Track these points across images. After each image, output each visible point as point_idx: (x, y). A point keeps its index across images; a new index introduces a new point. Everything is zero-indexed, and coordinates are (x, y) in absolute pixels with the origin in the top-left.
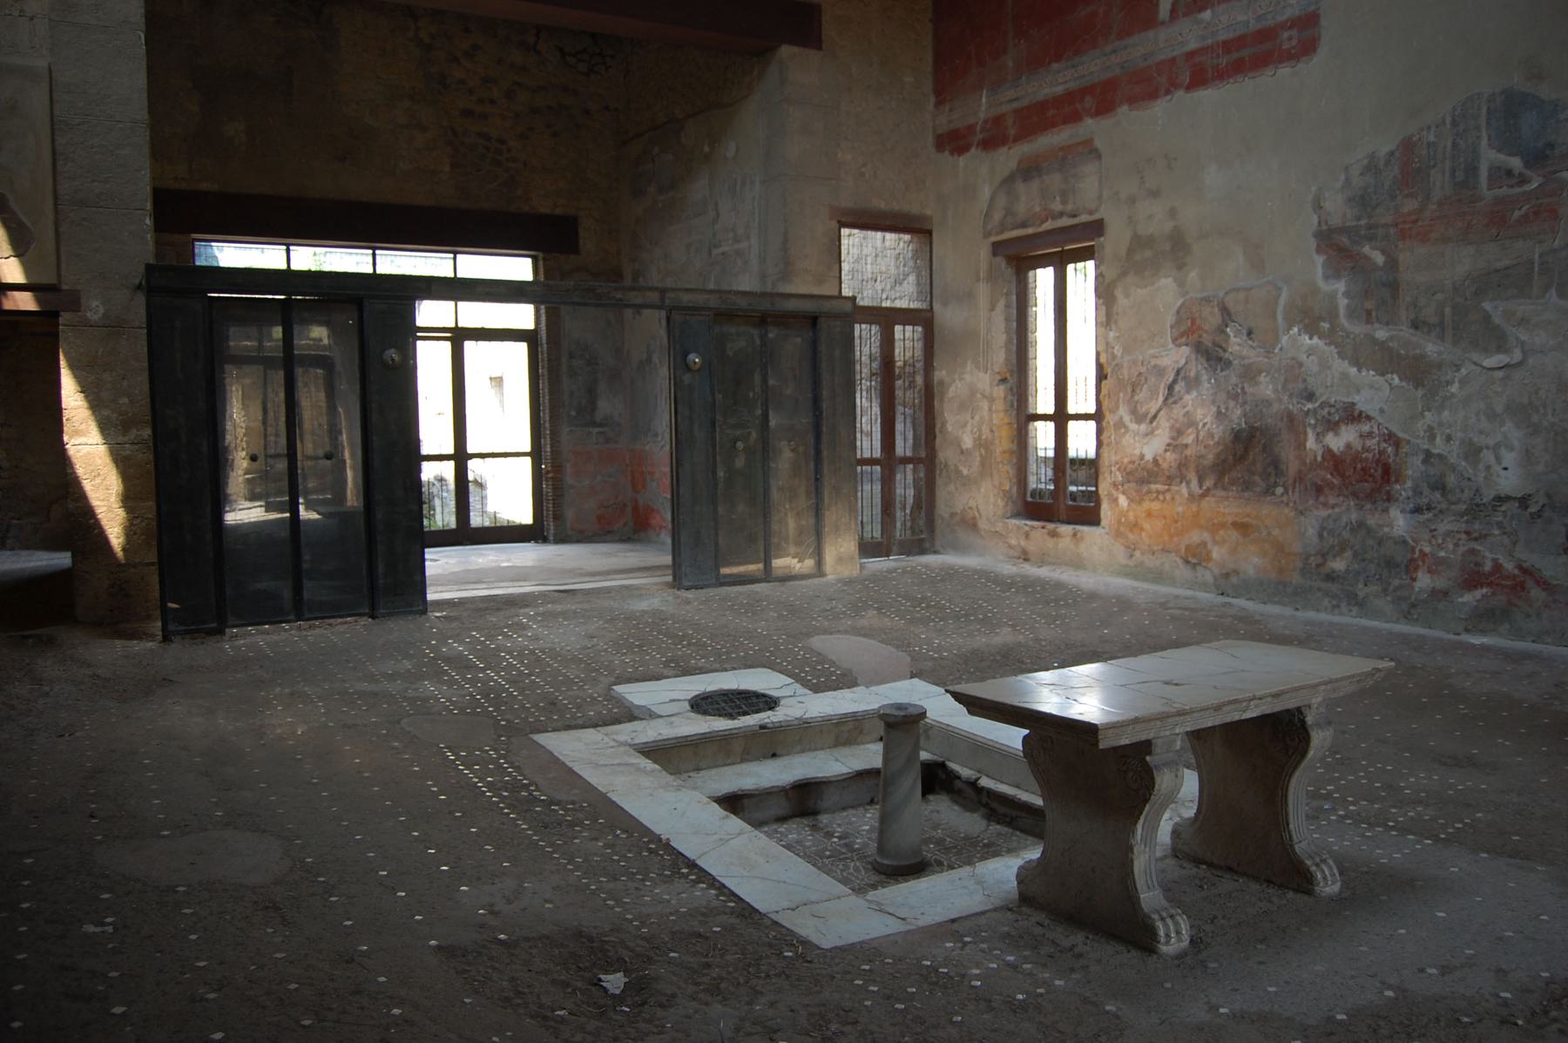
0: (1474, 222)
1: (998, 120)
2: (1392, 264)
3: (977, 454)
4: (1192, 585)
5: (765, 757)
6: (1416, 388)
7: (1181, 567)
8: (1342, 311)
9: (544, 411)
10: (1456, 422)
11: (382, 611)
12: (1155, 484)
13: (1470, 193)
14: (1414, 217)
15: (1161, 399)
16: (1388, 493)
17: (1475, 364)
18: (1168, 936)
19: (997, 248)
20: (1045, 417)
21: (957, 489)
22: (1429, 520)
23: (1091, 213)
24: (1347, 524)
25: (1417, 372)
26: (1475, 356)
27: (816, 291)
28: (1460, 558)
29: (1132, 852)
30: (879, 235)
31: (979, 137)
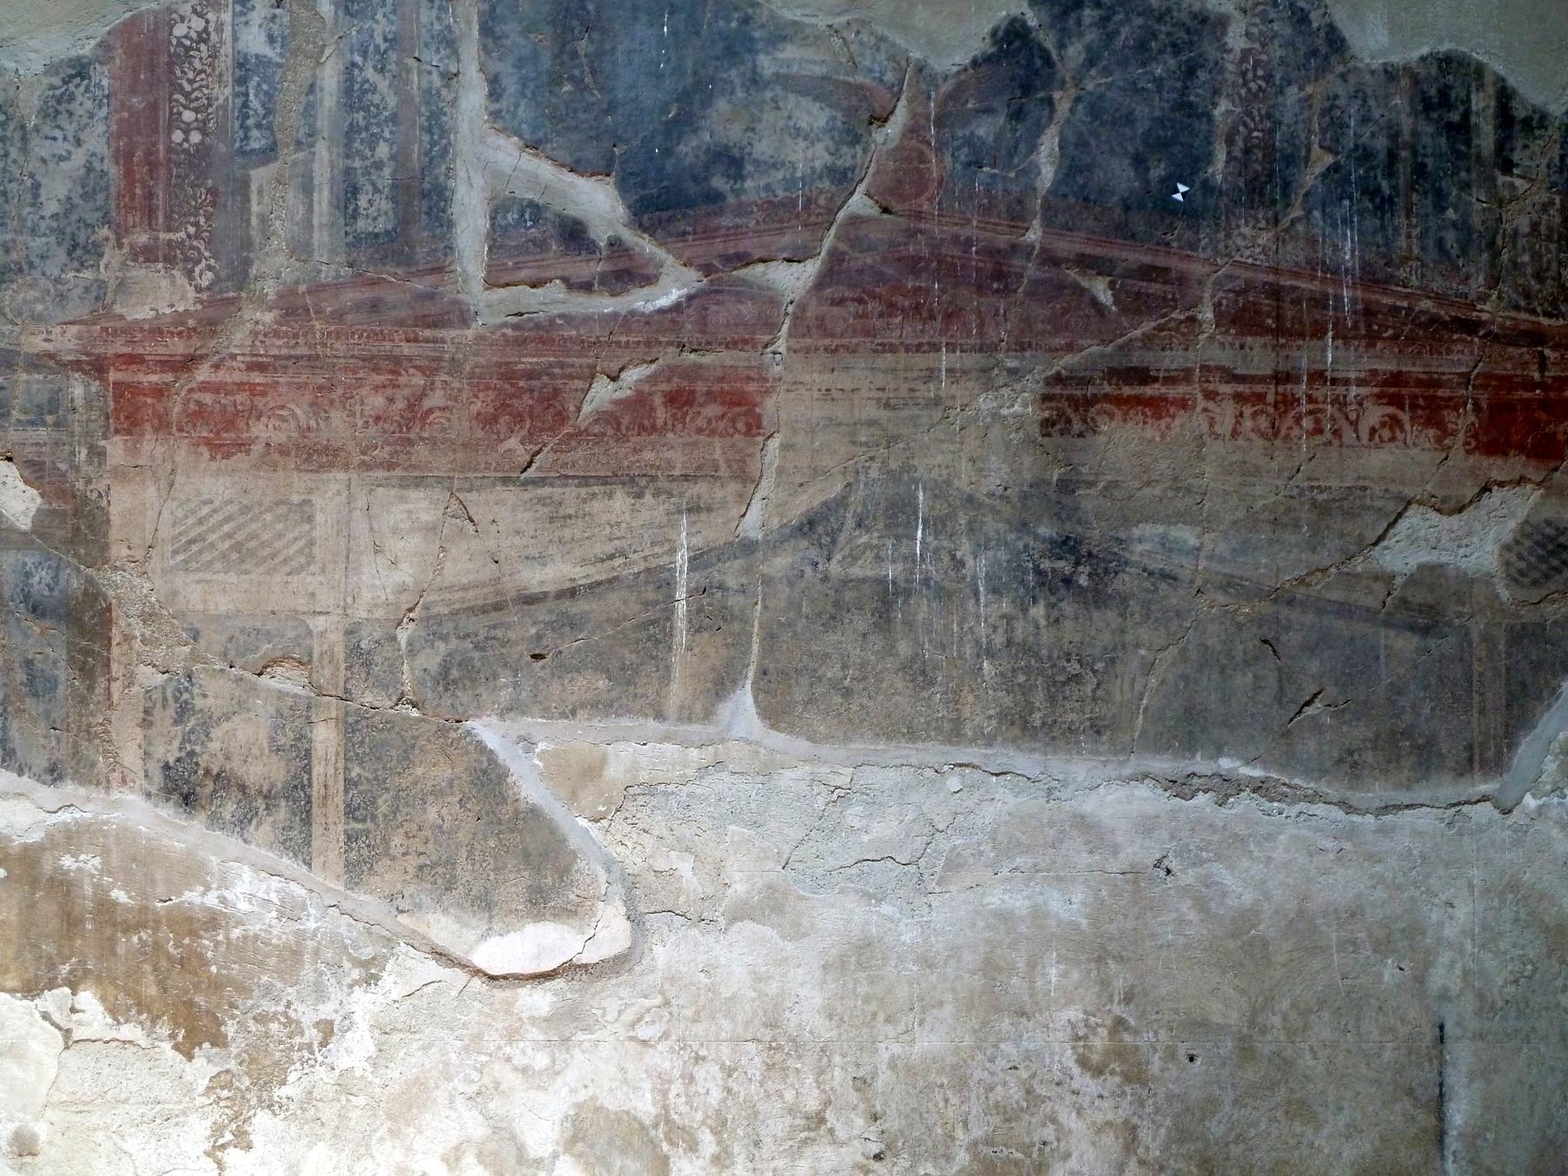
0: (436, 399)
13: (420, 285)
14: (178, 347)
17: (441, 956)
26: (442, 928)
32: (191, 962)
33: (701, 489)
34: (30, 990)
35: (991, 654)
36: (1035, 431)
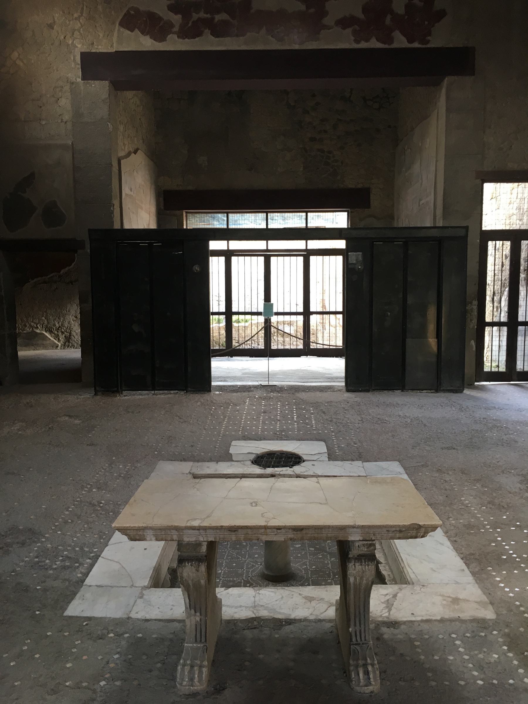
11: (189, 389)
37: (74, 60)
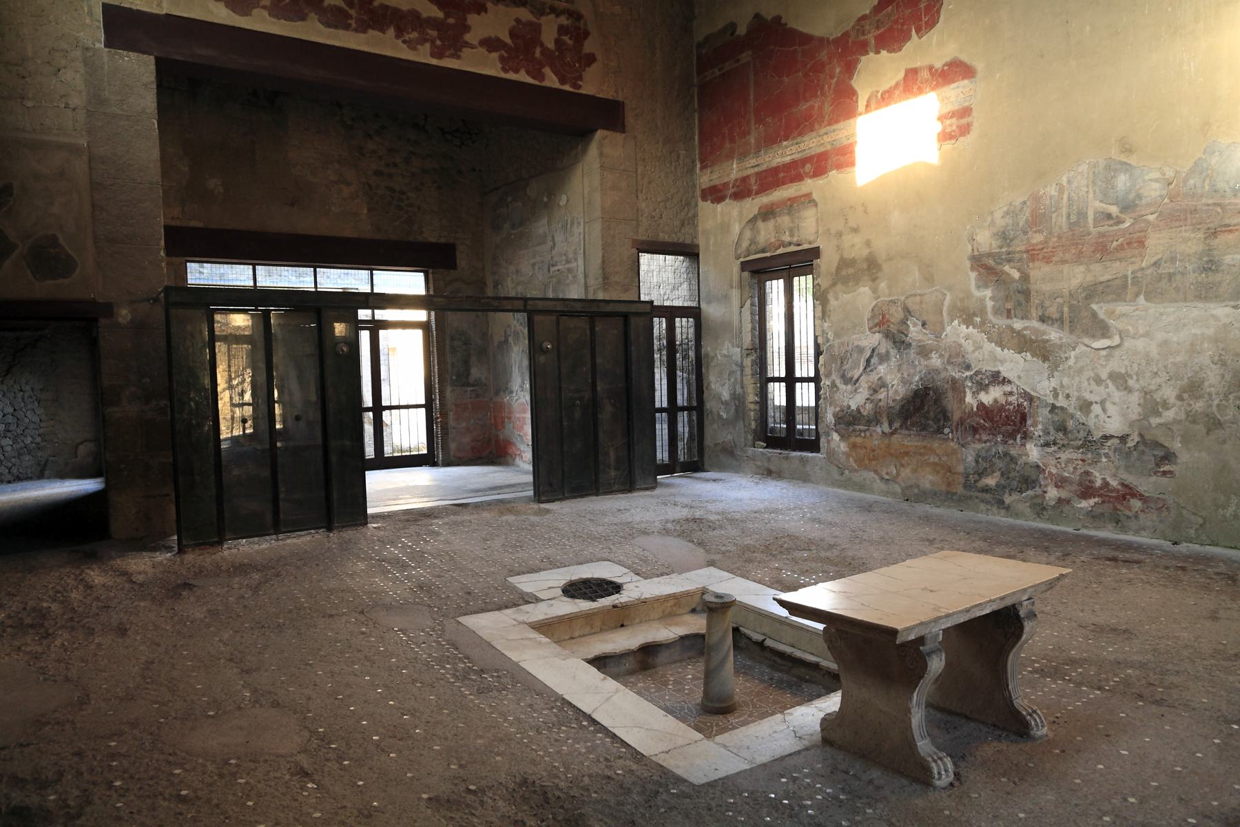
0: (1084, 249)
1: (744, 180)
2: (1025, 278)
3: (733, 404)
4: (886, 494)
5: (616, 627)
6: (1044, 362)
7: (878, 481)
8: (989, 310)
9: (434, 376)
10: (1073, 385)
12: (859, 425)
14: (1041, 247)
15: (862, 368)
16: (1025, 433)
18: (939, 773)
19: (744, 266)
20: (779, 380)
21: (719, 427)
22: (1055, 452)
23: (810, 243)
24: (996, 453)
25: (1043, 352)
26: (1086, 340)
27: (625, 297)
28: (1078, 478)
29: (910, 713)
30: (662, 257)
31: (731, 191)
32: (1045, 348)
33: (1133, 259)
34: (1020, 353)
35: (1192, 284)
36: (1202, 240)
37: (90, 13)
